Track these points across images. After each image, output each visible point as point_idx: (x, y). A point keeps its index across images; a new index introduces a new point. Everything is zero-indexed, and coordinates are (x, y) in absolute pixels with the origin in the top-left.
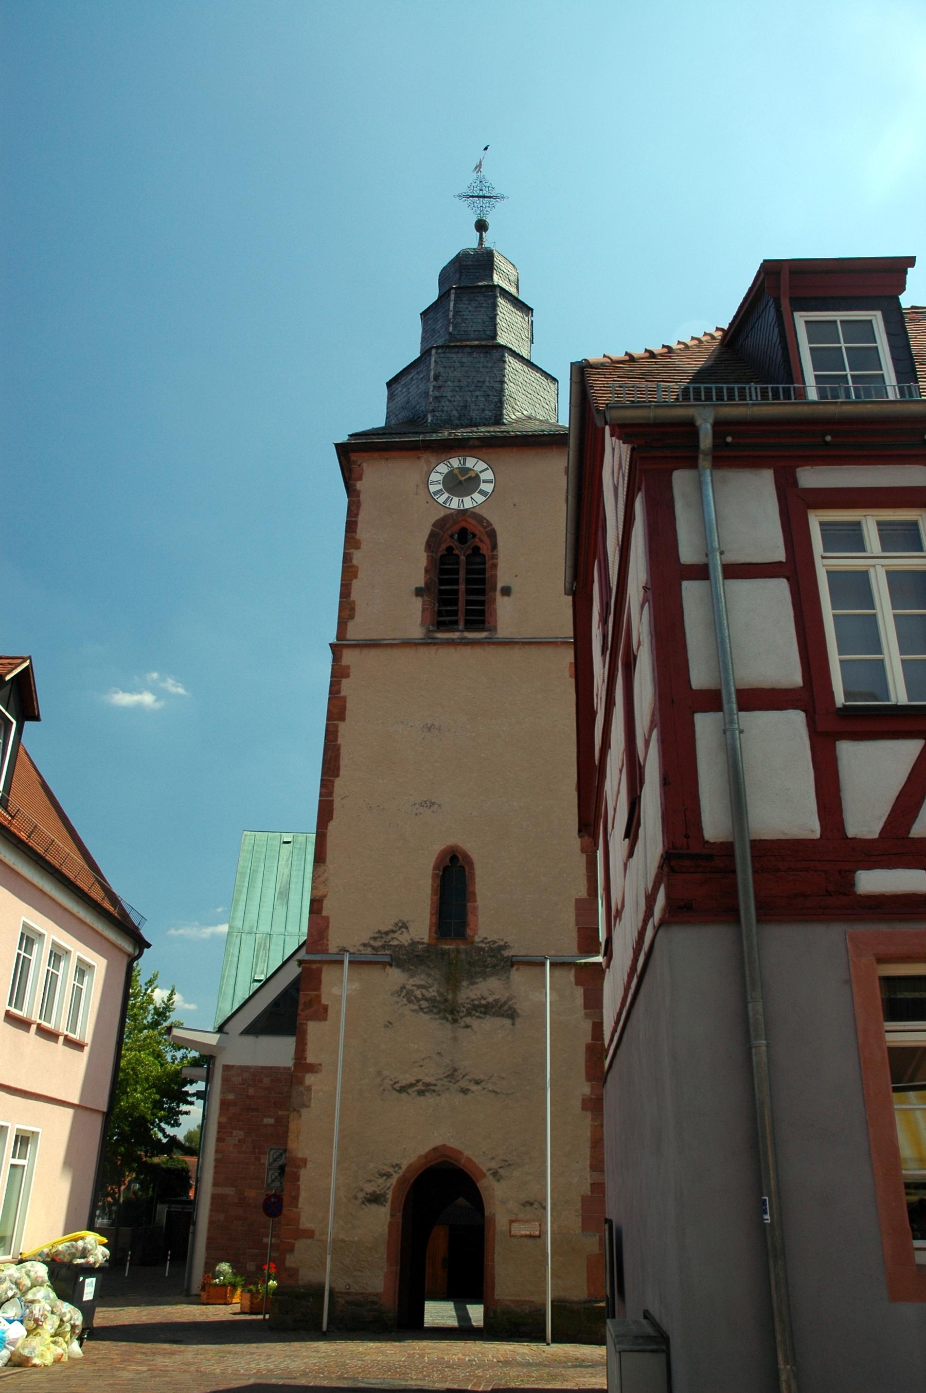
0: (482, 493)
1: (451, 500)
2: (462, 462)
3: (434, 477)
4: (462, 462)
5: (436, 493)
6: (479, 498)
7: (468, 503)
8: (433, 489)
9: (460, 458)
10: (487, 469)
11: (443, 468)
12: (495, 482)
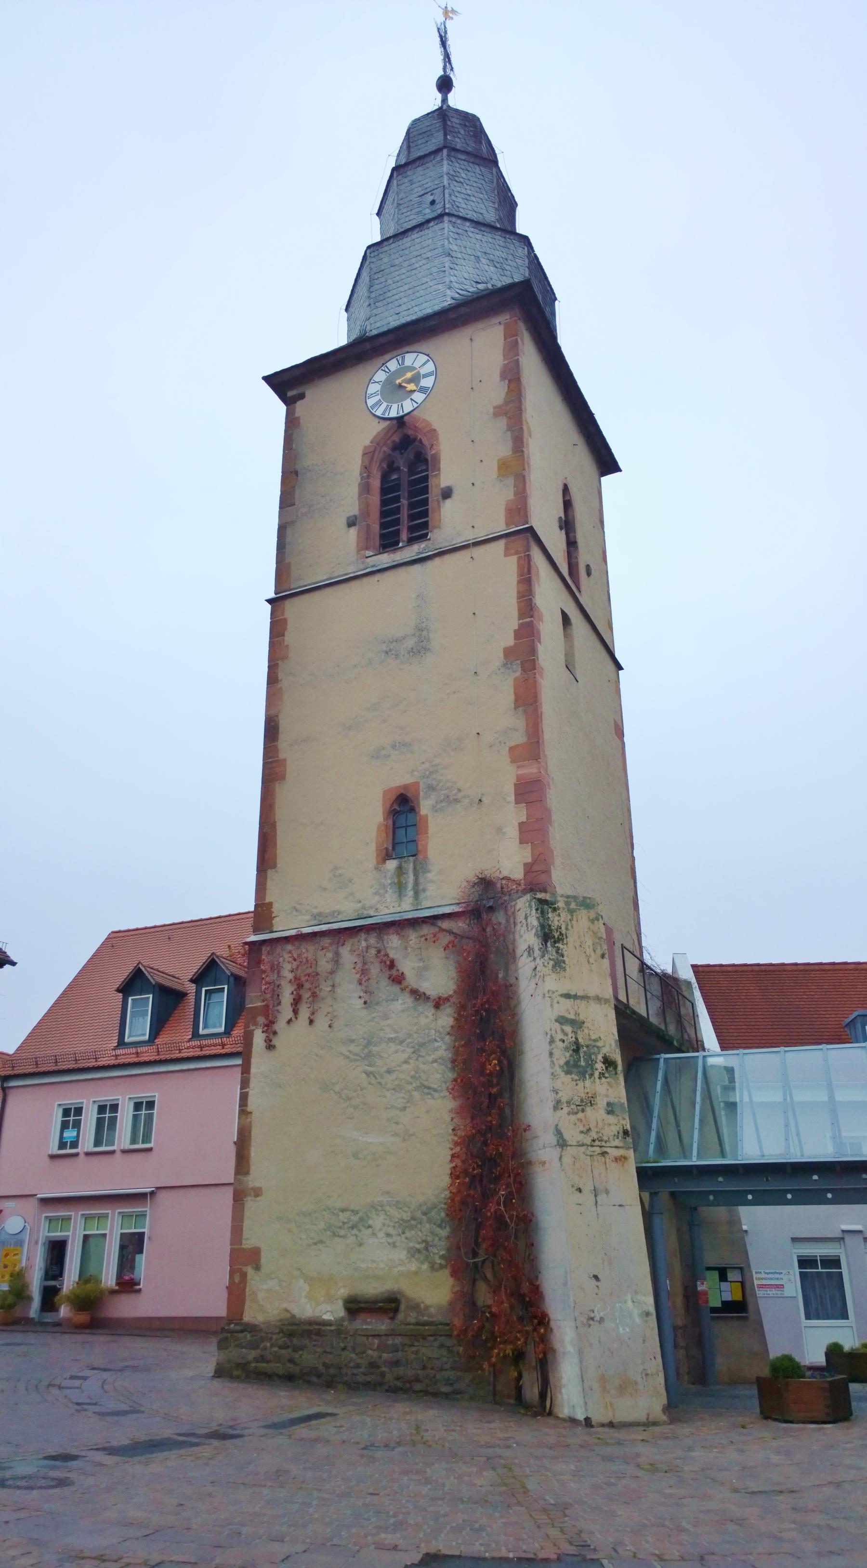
0: (423, 390)
2: (400, 362)
4: (400, 362)
6: (419, 397)
7: (408, 407)
10: (428, 361)
11: (381, 376)
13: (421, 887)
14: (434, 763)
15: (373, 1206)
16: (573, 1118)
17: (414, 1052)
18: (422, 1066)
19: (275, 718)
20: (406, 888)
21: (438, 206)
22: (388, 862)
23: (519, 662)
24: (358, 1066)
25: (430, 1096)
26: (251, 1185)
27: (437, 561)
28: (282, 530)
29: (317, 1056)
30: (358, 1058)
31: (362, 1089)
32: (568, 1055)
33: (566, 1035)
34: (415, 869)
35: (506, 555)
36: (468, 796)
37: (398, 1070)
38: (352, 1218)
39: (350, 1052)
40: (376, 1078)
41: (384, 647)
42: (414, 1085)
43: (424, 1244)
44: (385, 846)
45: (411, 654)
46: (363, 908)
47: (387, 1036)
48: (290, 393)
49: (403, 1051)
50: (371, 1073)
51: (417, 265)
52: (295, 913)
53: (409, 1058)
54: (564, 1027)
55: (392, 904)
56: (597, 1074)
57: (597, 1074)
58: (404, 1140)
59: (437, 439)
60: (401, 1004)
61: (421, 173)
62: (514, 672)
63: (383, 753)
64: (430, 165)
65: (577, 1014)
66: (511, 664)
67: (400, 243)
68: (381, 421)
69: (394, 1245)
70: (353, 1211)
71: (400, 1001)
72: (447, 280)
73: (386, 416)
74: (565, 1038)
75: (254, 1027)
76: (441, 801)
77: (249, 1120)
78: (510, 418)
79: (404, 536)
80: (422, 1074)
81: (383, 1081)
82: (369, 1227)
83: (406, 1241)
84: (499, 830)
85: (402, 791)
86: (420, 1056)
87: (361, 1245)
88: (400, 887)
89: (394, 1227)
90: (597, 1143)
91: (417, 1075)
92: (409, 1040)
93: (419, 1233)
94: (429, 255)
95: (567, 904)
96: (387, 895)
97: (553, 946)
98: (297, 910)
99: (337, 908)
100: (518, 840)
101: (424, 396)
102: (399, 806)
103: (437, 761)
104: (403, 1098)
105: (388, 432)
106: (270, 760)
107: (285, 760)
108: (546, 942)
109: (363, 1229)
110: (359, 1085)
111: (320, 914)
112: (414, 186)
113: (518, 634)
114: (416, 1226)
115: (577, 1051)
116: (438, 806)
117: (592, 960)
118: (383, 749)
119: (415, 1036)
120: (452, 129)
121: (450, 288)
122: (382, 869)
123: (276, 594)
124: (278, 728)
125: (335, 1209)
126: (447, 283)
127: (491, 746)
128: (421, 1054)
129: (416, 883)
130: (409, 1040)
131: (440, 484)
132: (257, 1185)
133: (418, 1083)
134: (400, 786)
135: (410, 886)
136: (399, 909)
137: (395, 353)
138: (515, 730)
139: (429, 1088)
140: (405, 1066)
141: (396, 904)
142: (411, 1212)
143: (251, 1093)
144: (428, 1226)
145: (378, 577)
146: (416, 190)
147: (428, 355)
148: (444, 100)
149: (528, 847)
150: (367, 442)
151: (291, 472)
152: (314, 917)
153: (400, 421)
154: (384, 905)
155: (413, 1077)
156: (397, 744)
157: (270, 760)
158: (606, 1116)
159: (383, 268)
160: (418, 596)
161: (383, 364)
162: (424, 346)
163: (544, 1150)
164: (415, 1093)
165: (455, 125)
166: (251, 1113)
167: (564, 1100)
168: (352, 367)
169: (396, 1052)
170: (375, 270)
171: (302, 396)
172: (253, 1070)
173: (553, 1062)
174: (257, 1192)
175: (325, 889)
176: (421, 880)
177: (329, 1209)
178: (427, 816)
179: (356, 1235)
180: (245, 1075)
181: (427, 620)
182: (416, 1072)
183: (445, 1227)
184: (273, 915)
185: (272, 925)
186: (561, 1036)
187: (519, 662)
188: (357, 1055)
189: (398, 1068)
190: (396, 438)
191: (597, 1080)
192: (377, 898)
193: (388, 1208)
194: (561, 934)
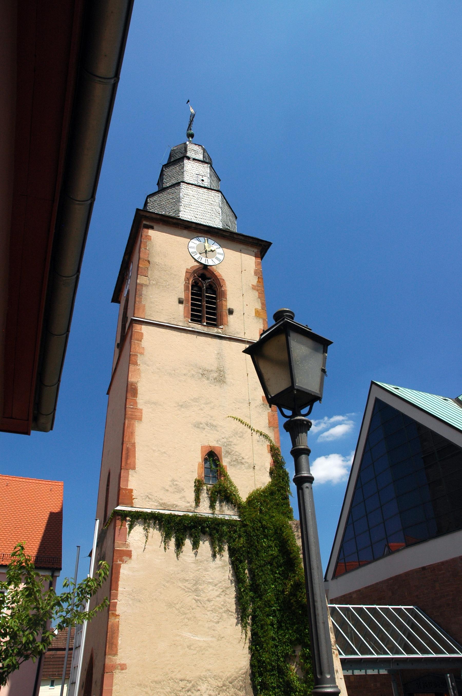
14: (228, 440)
15: (200, 678)
17: (223, 591)
18: (227, 600)
19: (135, 385)
24: (190, 595)
25: (232, 617)
26: (118, 662)
29: (164, 586)
30: (190, 591)
31: (193, 609)
36: (248, 463)
38: (187, 685)
39: (185, 587)
40: (201, 603)
41: (200, 371)
42: (223, 610)
45: (216, 381)
49: (216, 590)
50: (198, 600)
52: (147, 499)
53: (220, 594)
58: (218, 640)
63: (201, 426)
70: (188, 681)
73: (199, 260)
75: (121, 562)
76: (234, 461)
78: (259, 293)
81: (205, 606)
82: (199, 690)
86: (226, 594)
89: (213, 690)
91: (225, 604)
93: (228, 694)
98: (149, 498)
99: (175, 503)
103: (230, 440)
104: (217, 616)
105: (197, 267)
106: (132, 407)
107: (141, 410)
109: (195, 692)
110: (191, 606)
111: (164, 504)
114: (226, 690)
116: (232, 463)
118: (201, 424)
124: (137, 390)
125: (177, 679)
127: (258, 441)
130: (220, 585)
131: (227, 305)
132: (122, 662)
133: (225, 609)
137: (203, 236)
140: (218, 599)
142: (223, 682)
143: (118, 602)
144: (232, 689)
150: (189, 268)
151: (146, 260)
152: (161, 505)
153: (205, 267)
155: (222, 605)
157: (132, 407)
160: (218, 354)
161: (197, 237)
164: (223, 614)
166: (119, 615)
168: (181, 229)
169: (213, 590)
175: (167, 490)
177: (173, 679)
182: (225, 603)
183: (243, 691)
184: (133, 497)
185: (132, 503)
188: (189, 589)
189: (213, 599)
190: (201, 272)
193: (209, 679)
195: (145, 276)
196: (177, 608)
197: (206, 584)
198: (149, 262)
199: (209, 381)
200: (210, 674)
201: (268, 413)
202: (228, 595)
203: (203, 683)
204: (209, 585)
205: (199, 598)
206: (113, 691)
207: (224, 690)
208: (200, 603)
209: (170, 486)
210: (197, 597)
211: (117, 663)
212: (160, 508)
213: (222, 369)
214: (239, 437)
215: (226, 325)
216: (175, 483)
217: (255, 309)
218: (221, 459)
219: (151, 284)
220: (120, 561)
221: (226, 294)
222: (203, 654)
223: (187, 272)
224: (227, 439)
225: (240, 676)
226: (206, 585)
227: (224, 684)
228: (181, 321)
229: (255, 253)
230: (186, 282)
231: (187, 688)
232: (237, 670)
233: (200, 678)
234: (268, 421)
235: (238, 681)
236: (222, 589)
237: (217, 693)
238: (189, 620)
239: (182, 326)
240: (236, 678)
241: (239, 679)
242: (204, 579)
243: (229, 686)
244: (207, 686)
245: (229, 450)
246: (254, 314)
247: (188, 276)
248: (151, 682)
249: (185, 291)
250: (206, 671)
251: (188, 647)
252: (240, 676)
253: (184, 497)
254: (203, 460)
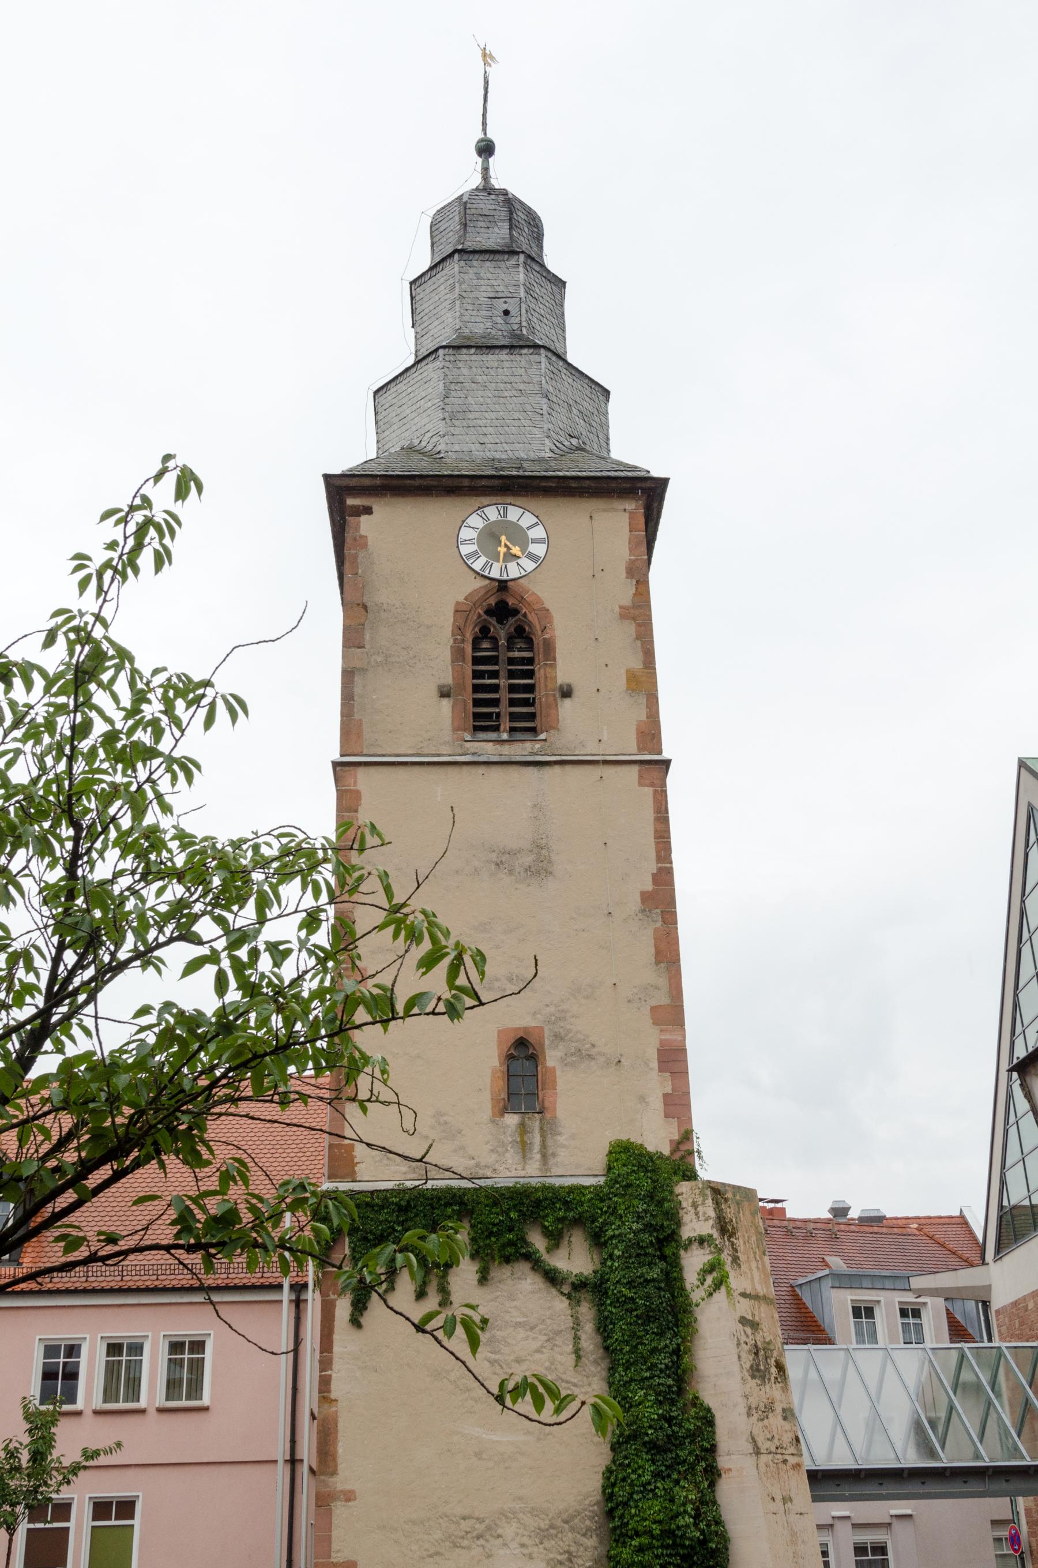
0: (532, 557)
1: (491, 565)
3: (466, 534)
5: (470, 555)
6: (529, 565)
7: (513, 571)
8: (465, 550)
9: (499, 506)
10: (536, 524)
12: (546, 541)
13: (550, 1151)
14: (560, 1008)
15: (503, 1513)
16: (761, 1424)
17: (548, 1340)
18: (559, 1358)
19: (350, 914)
20: (531, 1150)
21: (512, 320)
22: (506, 1115)
23: (659, 911)
26: (340, 1487)
27: (557, 769)
28: (348, 675)
32: (751, 1358)
33: (748, 1336)
34: (541, 1128)
35: (641, 784)
37: (530, 1360)
40: (502, 1368)
41: (494, 856)
43: (567, 1555)
44: (502, 1096)
46: (477, 1165)
47: (514, 1319)
48: (350, 502)
49: (534, 1339)
50: (496, 1361)
51: (506, 394)
53: (542, 1347)
54: (745, 1328)
55: (514, 1167)
56: (773, 1379)
57: (773, 1379)
58: (539, 1439)
59: (551, 622)
60: (531, 1284)
61: (491, 270)
62: (653, 921)
64: (502, 264)
65: (753, 1315)
66: (650, 911)
67: (484, 357)
68: (478, 577)
69: (531, 1557)
70: (478, 1519)
71: (529, 1281)
72: (546, 426)
73: (486, 574)
74: (747, 1341)
76: (572, 1055)
77: (334, 1409)
79: (506, 724)
80: (559, 1366)
82: (499, 1536)
83: (545, 1552)
84: (642, 1099)
85: (522, 1035)
87: (489, 1556)
88: (524, 1148)
89: (530, 1536)
90: (779, 1451)
91: (553, 1367)
92: (541, 1327)
93: (562, 1544)
94: (522, 387)
95: (734, 1195)
96: (507, 1155)
97: (729, 1240)
100: (663, 1114)
101: (534, 565)
102: (515, 1050)
105: (483, 592)
108: (724, 1236)
109: (491, 1539)
112: (482, 282)
113: (654, 876)
114: (556, 1536)
115: (756, 1354)
116: (569, 1060)
117: (758, 1258)
118: (497, 980)
119: (549, 1322)
120: (517, 224)
121: (548, 437)
122: (500, 1123)
123: (342, 755)
125: (455, 1517)
126: (545, 429)
127: (629, 1001)
128: (557, 1343)
129: (544, 1146)
130: (541, 1327)
131: (556, 677)
132: (348, 1487)
134: (520, 1028)
135: (537, 1147)
136: (523, 1173)
137: (494, 499)
138: (657, 988)
139: (567, 1382)
140: (537, 1356)
141: (519, 1167)
142: (550, 1520)
143: (334, 1375)
144: (570, 1534)
145: (481, 770)
146: (483, 288)
147: (537, 517)
148: (486, 170)
149: (675, 1121)
151: (358, 605)
153: (503, 585)
154: (504, 1166)
155: (546, 1369)
156: (515, 978)
158: (782, 1422)
159: (461, 379)
160: (535, 806)
161: (479, 508)
162: (533, 503)
163: (729, 1457)
165: (520, 220)
166: (336, 1400)
167: (753, 1406)
168: (437, 496)
169: (527, 1338)
170: (451, 377)
171: (368, 511)
172: (336, 1349)
173: (741, 1365)
174: (349, 1496)
176: (550, 1142)
177: (447, 1516)
178: (554, 1068)
179: (483, 1546)
180: (325, 1354)
181: (547, 837)
182: (552, 1364)
183: (591, 1536)
184: (356, 1160)
185: (354, 1173)
186: (743, 1338)
187: (659, 911)
189: (528, 1358)
190: (492, 601)
191: (774, 1385)
192: (494, 1156)
193: (521, 1516)
194: (733, 1228)
195: (358, 647)
196: (452, 1379)
197: (511, 1326)
198: (365, 607)
199: (513, 878)
200: (523, 1505)
201: (656, 930)
202: (560, 1346)
203: (508, 1523)
204: (519, 1329)
205: (497, 1357)
206: (333, 1539)
207: (552, 1535)
208: (498, 1367)
209: (432, 1128)
210: (493, 1356)
211: (338, 1489)
212: (412, 1176)
213: (544, 842)
214: (584, 998)
215: (554, 728)
216: (442, 1120)
217: (627, 671)
218: (544, 1053)
219: (373, 663)
220: (334, 1294)
221: (555, 648)
222: (506, 1468)
223: (456, 611)
224: (556, 1006)
225: (585, 1510)
226: (512, 1329)
227: (552, 1524)
228: (445, 743)
229: (630, 513)
230: (455, 640)
231: (476, 1532)
232: (579, 1498)
233: (502, 1514)
234: (652, 950)
235: (583, 1518)
236: (545, 1334)
237: (537, 1541)
238: (476, 1401)
239: (450, 755)
240: (579, 1513)
241: (583, 1515)
242: (507, 1317)
243: (562, 1527)
244: (517, 1528)
245: (561, 1030)
246: (622, 682)
247: (461, 622)
248: (405, 1522)
249: (452, 662)
250: (514, 1500)
251: (476, 1454)
252: (585, 1510)
253: (462, 1148)
254: (503, 1059)
